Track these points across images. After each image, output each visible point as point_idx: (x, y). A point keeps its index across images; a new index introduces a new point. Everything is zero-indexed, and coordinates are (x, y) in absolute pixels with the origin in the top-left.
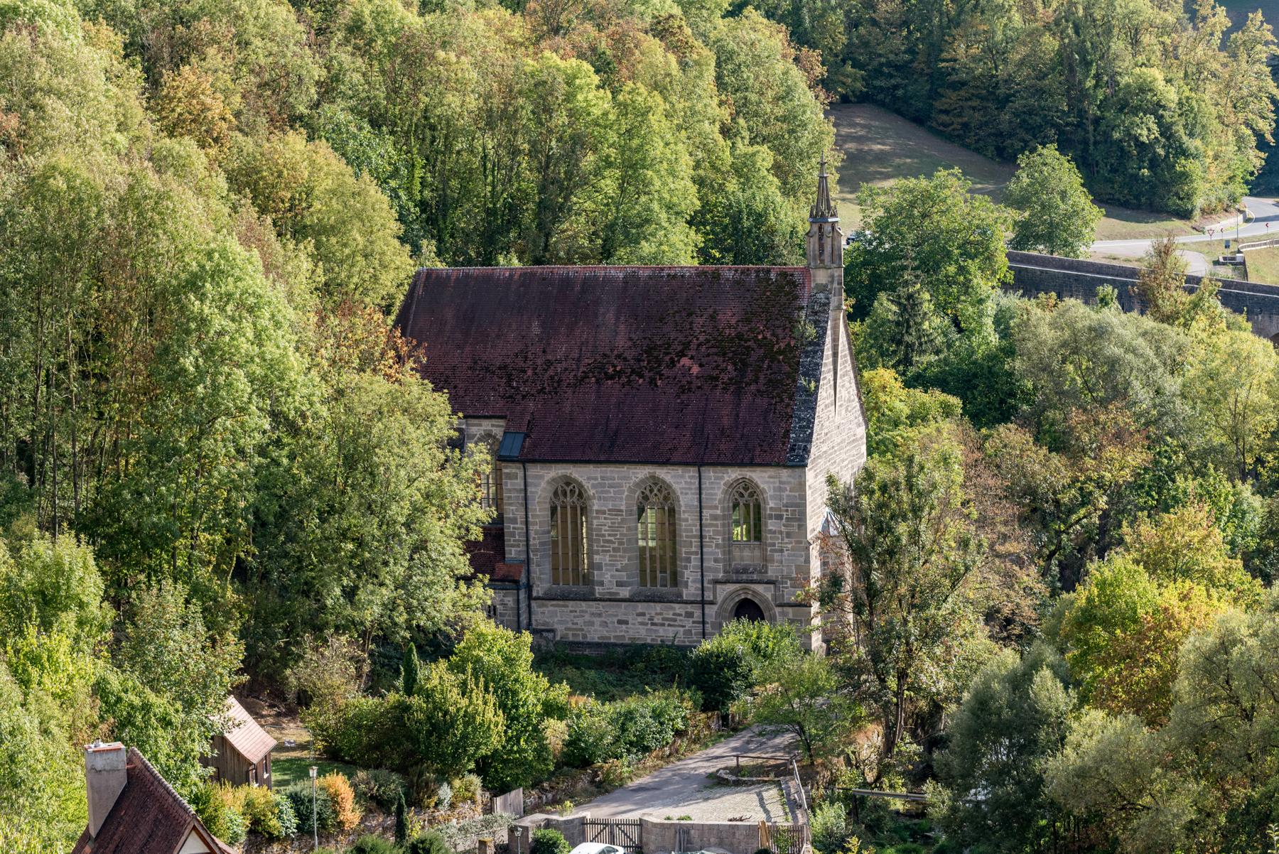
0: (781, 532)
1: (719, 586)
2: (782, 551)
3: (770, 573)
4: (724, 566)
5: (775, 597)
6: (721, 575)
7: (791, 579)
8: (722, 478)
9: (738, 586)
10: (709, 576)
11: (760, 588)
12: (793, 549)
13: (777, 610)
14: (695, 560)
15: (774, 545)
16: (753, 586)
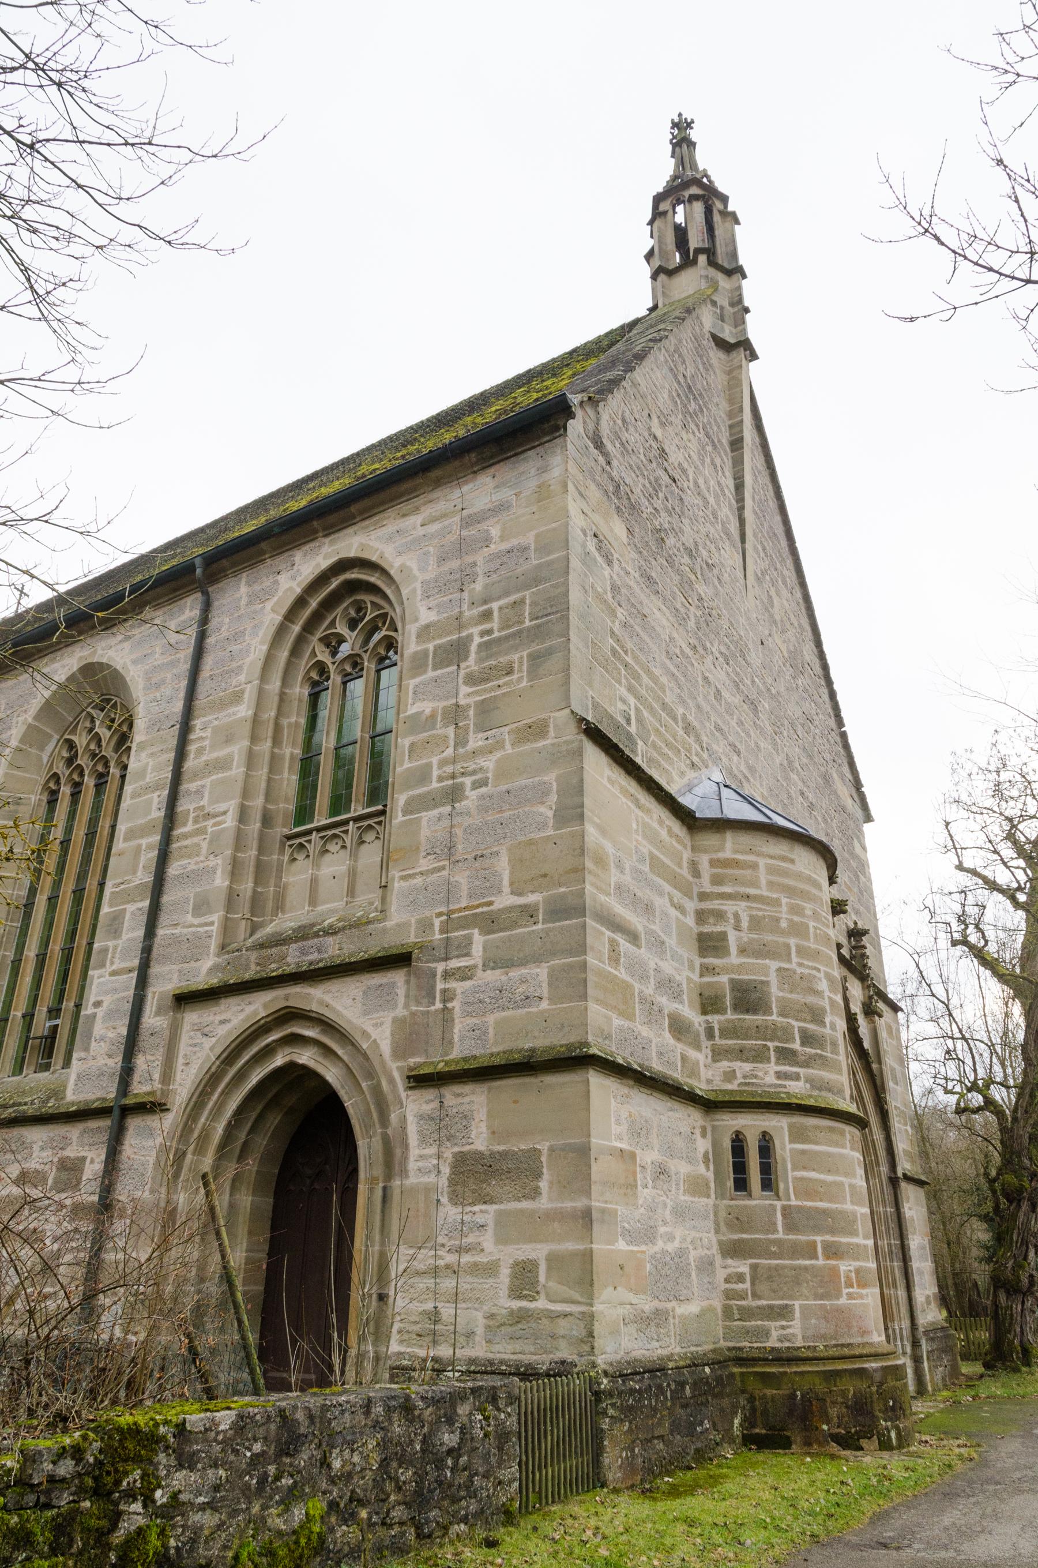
0: (455, 714)
1: (192, 1017)
2: (454, 794)
3: (396, 916)
4: (227, 927)
5: (408, 1036)
6: (204, 972)
7: (490, 922)
8: (269, 593)
9: (257, 1007)
10: (167, 980)
11: (342, 1001)
12: (502, 773)
13: (414, 1108)
14: (133, 932)
15: (423, 775)
16: (318, 997)
